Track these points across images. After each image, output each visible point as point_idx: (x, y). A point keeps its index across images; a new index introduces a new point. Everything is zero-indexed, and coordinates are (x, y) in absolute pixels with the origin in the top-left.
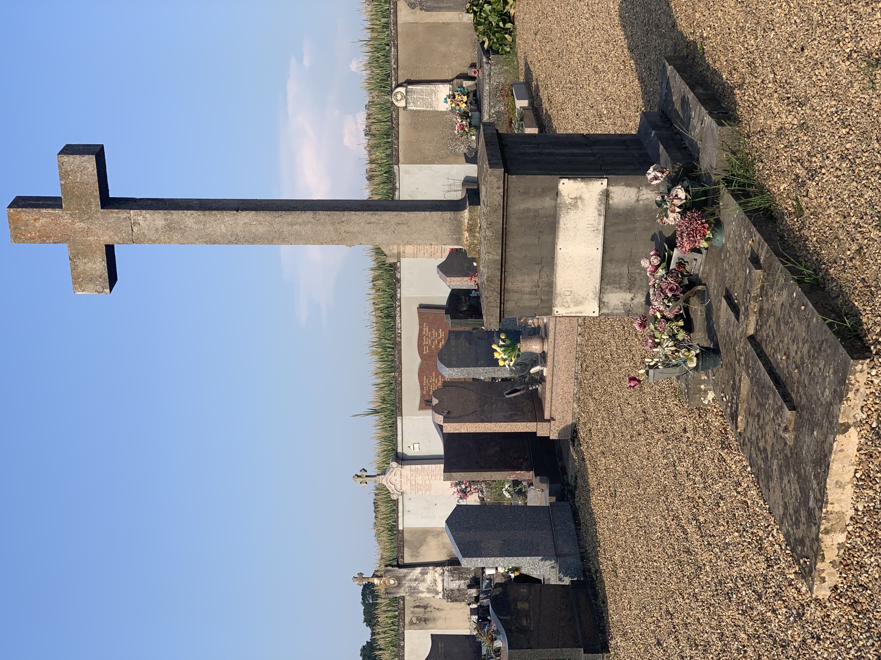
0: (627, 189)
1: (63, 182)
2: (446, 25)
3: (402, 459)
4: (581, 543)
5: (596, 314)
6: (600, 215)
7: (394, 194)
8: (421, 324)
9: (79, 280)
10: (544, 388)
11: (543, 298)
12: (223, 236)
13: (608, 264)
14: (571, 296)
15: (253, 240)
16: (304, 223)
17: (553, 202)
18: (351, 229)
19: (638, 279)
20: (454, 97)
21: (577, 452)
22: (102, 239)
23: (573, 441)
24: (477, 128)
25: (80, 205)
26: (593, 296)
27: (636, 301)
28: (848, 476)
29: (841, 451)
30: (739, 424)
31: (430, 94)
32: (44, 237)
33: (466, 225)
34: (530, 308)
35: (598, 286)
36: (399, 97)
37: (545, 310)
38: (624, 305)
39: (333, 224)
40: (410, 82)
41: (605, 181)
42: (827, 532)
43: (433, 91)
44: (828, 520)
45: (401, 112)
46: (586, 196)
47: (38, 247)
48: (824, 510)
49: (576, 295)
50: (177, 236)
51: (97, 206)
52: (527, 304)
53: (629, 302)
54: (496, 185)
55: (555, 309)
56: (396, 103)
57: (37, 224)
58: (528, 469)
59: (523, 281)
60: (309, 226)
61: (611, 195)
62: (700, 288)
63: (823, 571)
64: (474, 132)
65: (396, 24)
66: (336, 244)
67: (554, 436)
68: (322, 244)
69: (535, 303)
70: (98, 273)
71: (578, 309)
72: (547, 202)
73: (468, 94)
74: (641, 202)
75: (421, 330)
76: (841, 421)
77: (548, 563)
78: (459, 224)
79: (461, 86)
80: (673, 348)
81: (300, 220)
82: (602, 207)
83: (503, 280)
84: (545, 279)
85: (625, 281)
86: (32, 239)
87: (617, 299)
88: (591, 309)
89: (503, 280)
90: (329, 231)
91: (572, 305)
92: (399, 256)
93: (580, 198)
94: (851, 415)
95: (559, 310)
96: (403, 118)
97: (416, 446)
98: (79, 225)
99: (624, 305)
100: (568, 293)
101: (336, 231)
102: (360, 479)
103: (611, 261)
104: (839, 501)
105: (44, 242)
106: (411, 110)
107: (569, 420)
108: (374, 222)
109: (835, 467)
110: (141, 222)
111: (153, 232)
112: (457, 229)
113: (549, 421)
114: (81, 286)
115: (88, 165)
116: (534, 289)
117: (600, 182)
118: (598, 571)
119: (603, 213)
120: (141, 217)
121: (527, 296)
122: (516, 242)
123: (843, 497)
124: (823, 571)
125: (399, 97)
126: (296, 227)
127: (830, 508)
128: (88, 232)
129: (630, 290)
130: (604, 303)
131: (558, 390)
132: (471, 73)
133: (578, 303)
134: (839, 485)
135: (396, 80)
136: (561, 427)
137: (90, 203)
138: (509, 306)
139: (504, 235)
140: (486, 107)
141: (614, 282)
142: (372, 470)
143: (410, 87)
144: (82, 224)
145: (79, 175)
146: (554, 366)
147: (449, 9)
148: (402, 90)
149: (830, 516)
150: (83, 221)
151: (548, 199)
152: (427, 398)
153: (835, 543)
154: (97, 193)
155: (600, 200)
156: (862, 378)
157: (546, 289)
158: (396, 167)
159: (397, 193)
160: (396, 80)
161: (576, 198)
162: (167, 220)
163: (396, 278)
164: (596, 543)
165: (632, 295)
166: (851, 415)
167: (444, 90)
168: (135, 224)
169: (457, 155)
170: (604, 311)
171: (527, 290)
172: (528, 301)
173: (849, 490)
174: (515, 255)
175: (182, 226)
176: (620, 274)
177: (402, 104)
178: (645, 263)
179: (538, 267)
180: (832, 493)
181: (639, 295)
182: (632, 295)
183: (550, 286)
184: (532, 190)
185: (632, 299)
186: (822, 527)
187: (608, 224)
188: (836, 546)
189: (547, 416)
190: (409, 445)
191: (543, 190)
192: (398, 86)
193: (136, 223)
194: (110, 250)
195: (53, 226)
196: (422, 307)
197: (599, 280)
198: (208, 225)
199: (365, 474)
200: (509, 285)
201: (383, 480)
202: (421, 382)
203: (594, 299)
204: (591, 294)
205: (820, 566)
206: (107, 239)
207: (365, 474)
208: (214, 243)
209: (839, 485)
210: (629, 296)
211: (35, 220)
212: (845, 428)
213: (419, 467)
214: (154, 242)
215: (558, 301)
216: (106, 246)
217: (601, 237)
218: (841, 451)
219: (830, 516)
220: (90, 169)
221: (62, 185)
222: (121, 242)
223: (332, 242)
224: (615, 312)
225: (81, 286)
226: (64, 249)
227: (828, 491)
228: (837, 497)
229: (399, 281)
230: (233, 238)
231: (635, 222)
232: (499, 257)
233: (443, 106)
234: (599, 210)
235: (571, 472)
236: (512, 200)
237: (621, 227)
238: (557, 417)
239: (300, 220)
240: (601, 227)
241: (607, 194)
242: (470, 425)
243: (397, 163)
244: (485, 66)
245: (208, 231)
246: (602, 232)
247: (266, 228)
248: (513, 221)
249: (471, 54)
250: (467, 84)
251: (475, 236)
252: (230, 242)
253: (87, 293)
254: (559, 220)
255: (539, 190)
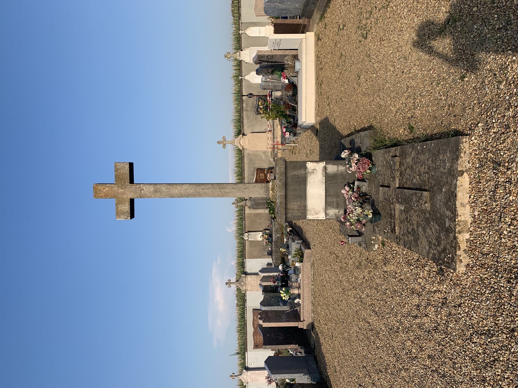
0: (333, 166)
1: (116, 173)
2: (260, 214)
3: (248, 369)
4: (319, 368)
5: (324, 218)
6: (323, 176)
7: (244, 269)
8: (254, 316)
9: (118, 214)
10: (300, 308)
11: (302, 212)
12: (176, 194)
13: (328, 197)
14: (314, 211)
15: (188, 196)
16: (209, 189)
17: (304, 172)
18: (226, 191)
19: (340, 203)
20: (263, 236)
21: (314, 333)
22: (129, 196)
23: (312, 329)
24: (271, 243)
25: (122, 182)
26: (323, 211)
27: (340, 213)
28: (466, 200)
29: (462, 186)
30: (397, 231)
31: (256, 235)
32: (106, 196)
33: (271, 188)
34: (297, 216)
35: (324, 206)
36: (246, 236)
37: (304, 217)
38: (336, 215)
39: (219, 189)
40: (249, 232)
41: (324, 163)
42: (460, 232)
43: (256, 234)
44: (460, 226)
45: (246, 241)
46: (317, 169)
47: (104, 199)
48: (457, 220)
49: (316, 210)
50: (158, 194)
51: (128, 183)
52: (296, 215)
53: (337, 213)
54: (282, 164)
55: (308, 216)
56: (245, 238)
57: (104, 191)
58: (296, 344)
59: (294, 205)
60: (210, 190)
61: (327, 168)
62: (367, 197)
63: (460, 255)
64: (270, 244)
65: (245, 214)
66: (220, 197)
67: (305, 328)
68: (215, 197)
69: (299, 214)
70: (126, 211)
71: (317, 216)
72: (302, 172)
73: (268, 235)
74: (339, 171)
75: (254, 318)
76: (459, 169)
77: (306, 376)
78: (268, 188)
79: (266, 232)
80: (361, 211)
81: (207, 187)
82: (324, 173)
83: (286, 204)
84: (303, 204)
85: (335, 204)
86: (102, 197)
87: (332, 212)
88: (322, 216)
89: (286, 204)
90: (218, 192)
91: (314, 214)
92: (246, 291)
93: (315, 169)
94: (464, 166)
95: (309, 217)
96: (247, 243)
97: (252, 363)
98: (121, 191)
99: (336, 215)
100: (312, 209)
101: (220, 192)
102: (232, 377)
103: (329, 196)
104: (464, 214)
105: (106, 198)
106: (250, 241)
107: (311, 321)
108: (235, 188)
109: (459, 195)
110: (145, 189)
111: (149, 193)
112: (267, 190)
113: (303, 321)
114: (119, 216)
115: (126, 166)
116: (298, 208)
117: (322, 163)
118: (327, 377)
119: (324, 175)
120: (145, 187)
121: (296, 211)
122: (290, 188)
123: (466, 212)
124: (460, 255)
125: (246, 236)
126: (205, 190)
127: (459, 218)
128: (124, 193)
129: (337, 208)
130: (327, 214)
131: (305, 308)
132: (268, 228)
133: (317, 213)
134: (463, 205)
135: (245, 231)
136: (308, 324)
137: (125, 182)
138: (289, 215)
139: (286, 185)
140: (274, 235)
141: (331, 205)
142: (234, 280)
143: (249, 233)
144: (122, 190)
145: (122, 170)
146: (303, 298)
147: (261, 208)
148: (247, 234)
149: (460, 223)
150: (122, 189)
151: (302, 170)
152: (256, 344)
153: (465, 239)
154: (128, 177)
155: (323, 170)
156: (466, 145)
157: (303, 208)
158: (245, 260)
159: (245, 269)
160: (245, 231)
161: (313, 169)
162: (154, 188)
163: (245, 299)
164: (325, 365)
165: (338, 210)
166: (464, 166)
167: (261, 233)
168: (142, 190)
169: (264, 255)
170: (328, 217)
171: (296, 208)
172: (297, 213)
173: (468, 207)
174: (290, 193)
175: (161, 190)
176: (333, 201)
177: (246, 238)
178: (343, 191)
179: (300, 199)
180: (460, 210)
181: (341, 210)
182: (338, 210)
183: (305, 206)
184: (296, 167)
185: (339, 212)
186: (457, 230)
187: (326, 180)
188: (465, 241)
189: (302, 320)
190: (250, 363)
191: (300, 167)
192: (245, 233)
193: (143, 190)
194: (132, 201)
195: (110, 191)
196: (254, 310)
197: (324, 204)
198: (170, 190)
199: (234, 375)
200: (289, 207)
201: (240, 377)
202: (254, 338)
203: (323, 212)
204: (322, 210)
205: (458, 253)
206: (131, 196)
207: (234, 375)
208: (173, 197)
209: (463, 205)
210: (337, 211)
211: (104, 189)
212: (462, 173)
213: (253, 372)
214: (149, 197)
215: (308, 213)
216: (131, 199)
217: (324, 185)
218: (462, 186)
219: (460, 223)
220: (127, 168)
221: (115, 174)
222: (136, 197)
223: (219, 196)
224: (332, 218)
225: (119, 216)
226: (114, 201)
227: (458, 209)
228: (462, 212)
229: (246, 300)
230: (180, 195)
231: (337, 179)
232: (284, 194)
233: (260, 239)
234: (323, 174)
235: (312, 343)
236: (288, 171)
237: (332, 182)
238: (306, 319)
239: (207, 187)
240: (324, 181)
241: (325, 168)
242: (273, 323)
243: (245, 259)
244: (273, 222)
245: (171, 192)
246: (324, 183)
247: (193, 191)
248: (289, 180)
249: (268, 223)
250: (267, 231)
251: (274, 192)
252: (179, 197)
253: (122, 219)
254: (307, 178)
255: (299, 167)
